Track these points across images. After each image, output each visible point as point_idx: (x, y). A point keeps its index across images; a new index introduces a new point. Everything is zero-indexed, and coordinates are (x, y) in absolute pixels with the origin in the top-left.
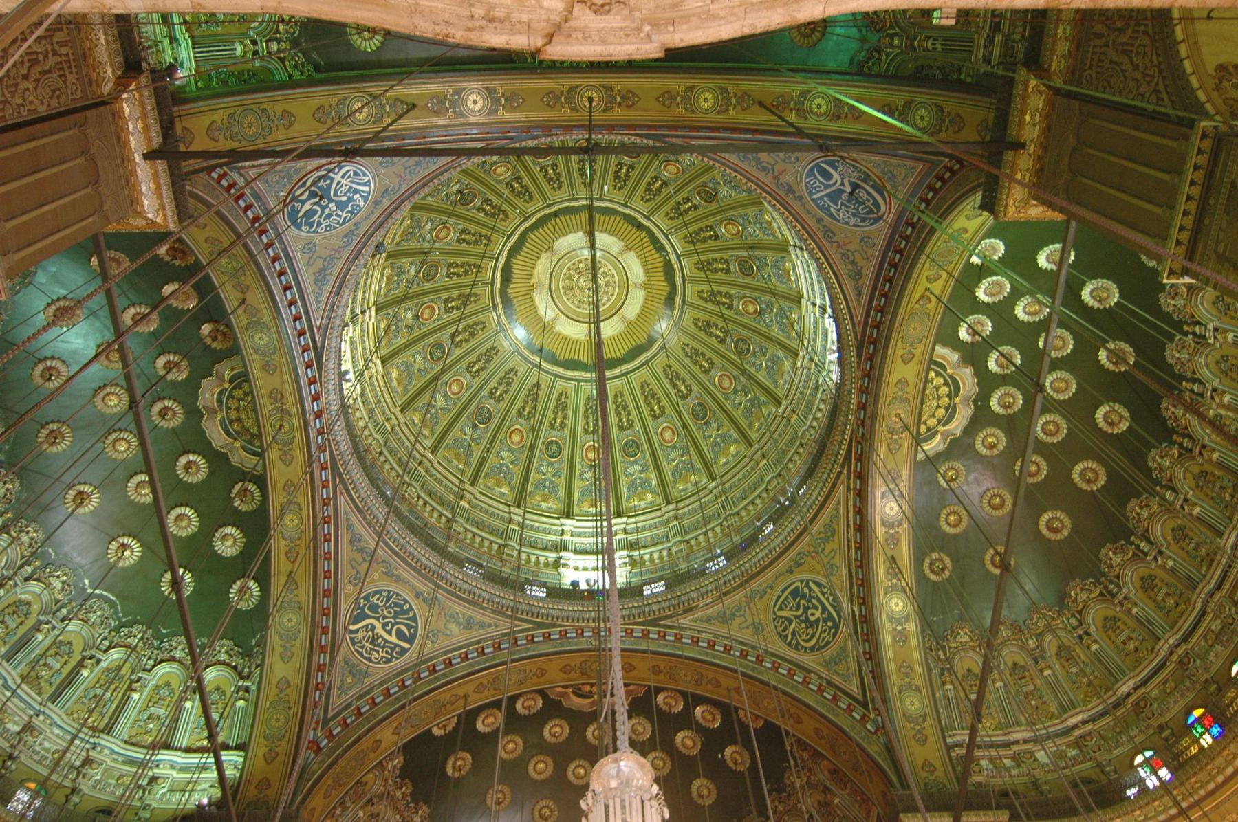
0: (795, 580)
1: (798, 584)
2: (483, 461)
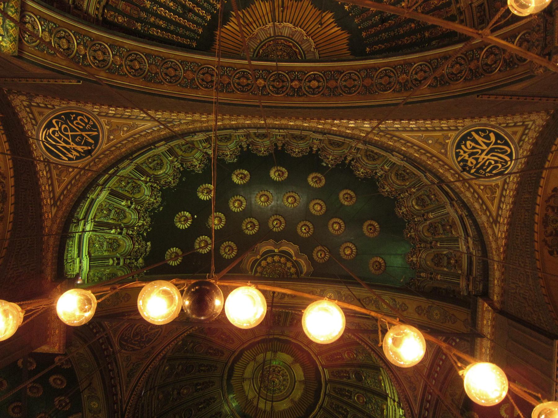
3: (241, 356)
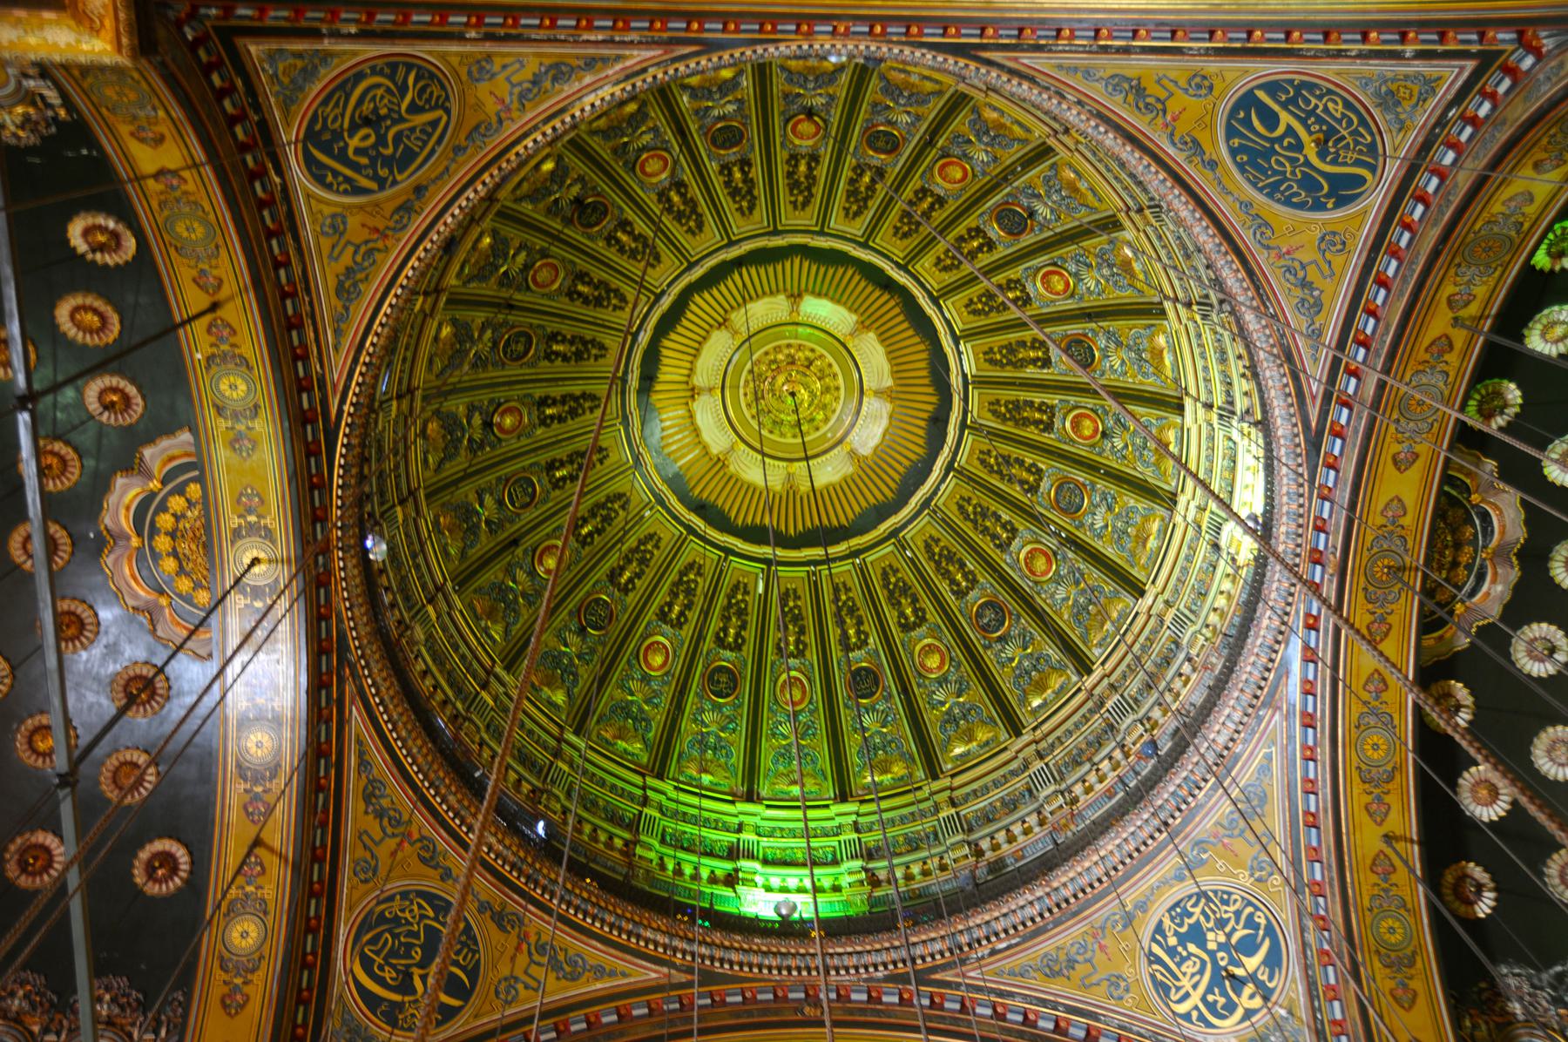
0: (407, 180)
1: (399, 178)
2: (1029, 162)
3: (678, 321)
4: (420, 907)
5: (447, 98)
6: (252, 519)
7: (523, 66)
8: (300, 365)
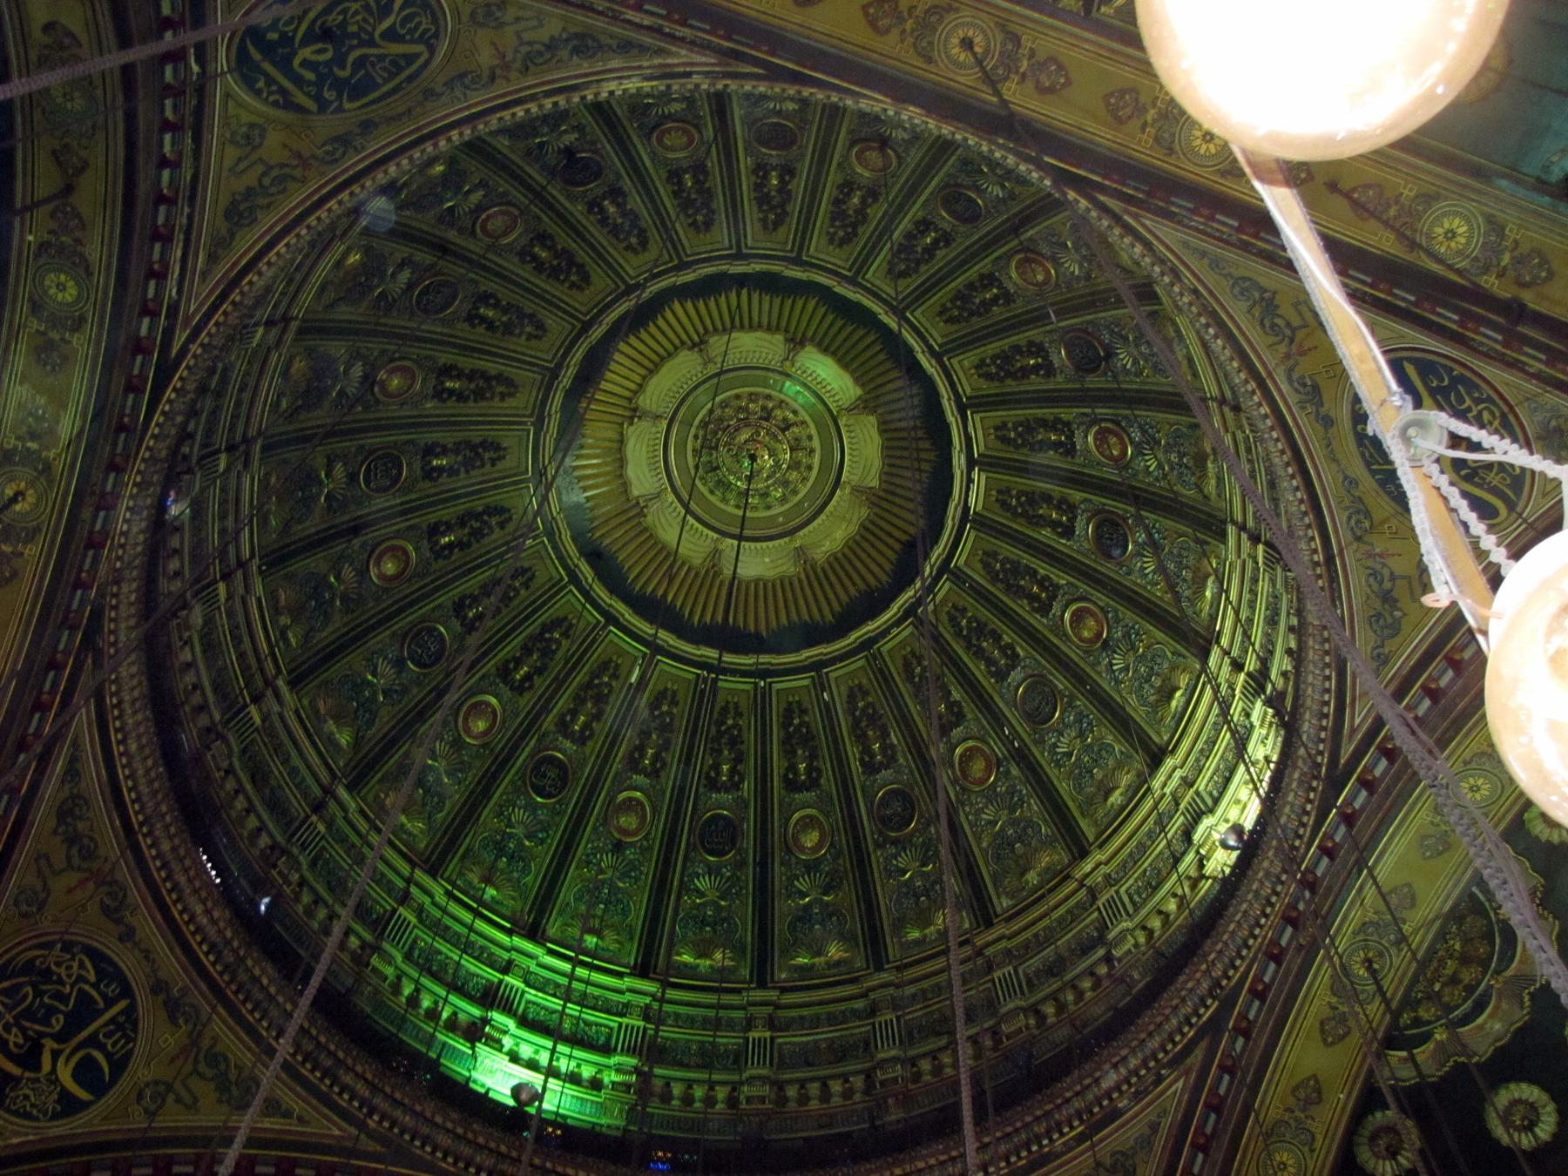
1: (347, 106)
4: (82, 965)
5: (436, 36)
6: (32, 445)
7: (541, 25)
8: (152, 283)
